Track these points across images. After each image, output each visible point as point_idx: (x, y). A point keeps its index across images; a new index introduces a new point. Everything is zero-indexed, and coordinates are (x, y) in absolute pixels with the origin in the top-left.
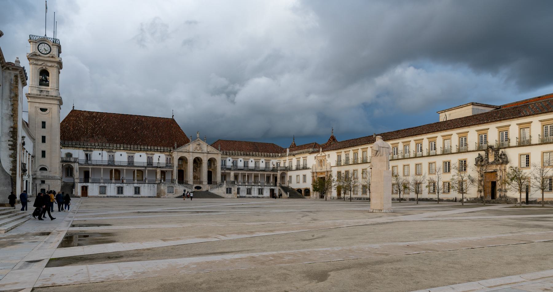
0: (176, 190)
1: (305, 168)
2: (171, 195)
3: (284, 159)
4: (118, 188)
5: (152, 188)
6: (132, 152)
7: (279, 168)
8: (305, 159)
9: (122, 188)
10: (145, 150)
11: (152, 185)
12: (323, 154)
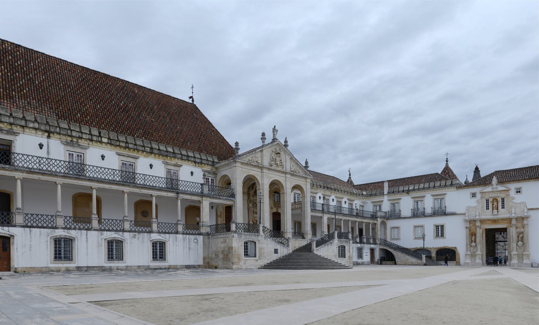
0: (261, 249)
1: (441, 212)
2: (251, 262)
3: (377, 199)
4: (110, 243)
5: (193, 245)
6: (131, 153)
7: (379, 214)
8: (441, 198)
9: (120, 243)
10: (160, 154)
11: (192, 237)
12: (500, 188)
